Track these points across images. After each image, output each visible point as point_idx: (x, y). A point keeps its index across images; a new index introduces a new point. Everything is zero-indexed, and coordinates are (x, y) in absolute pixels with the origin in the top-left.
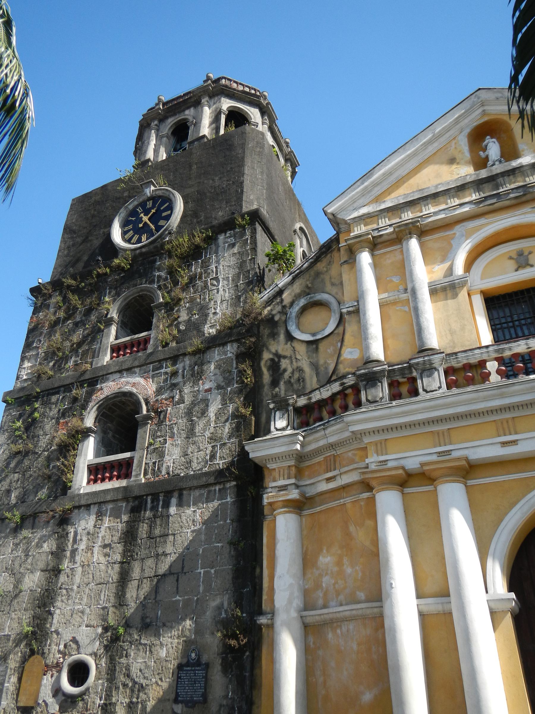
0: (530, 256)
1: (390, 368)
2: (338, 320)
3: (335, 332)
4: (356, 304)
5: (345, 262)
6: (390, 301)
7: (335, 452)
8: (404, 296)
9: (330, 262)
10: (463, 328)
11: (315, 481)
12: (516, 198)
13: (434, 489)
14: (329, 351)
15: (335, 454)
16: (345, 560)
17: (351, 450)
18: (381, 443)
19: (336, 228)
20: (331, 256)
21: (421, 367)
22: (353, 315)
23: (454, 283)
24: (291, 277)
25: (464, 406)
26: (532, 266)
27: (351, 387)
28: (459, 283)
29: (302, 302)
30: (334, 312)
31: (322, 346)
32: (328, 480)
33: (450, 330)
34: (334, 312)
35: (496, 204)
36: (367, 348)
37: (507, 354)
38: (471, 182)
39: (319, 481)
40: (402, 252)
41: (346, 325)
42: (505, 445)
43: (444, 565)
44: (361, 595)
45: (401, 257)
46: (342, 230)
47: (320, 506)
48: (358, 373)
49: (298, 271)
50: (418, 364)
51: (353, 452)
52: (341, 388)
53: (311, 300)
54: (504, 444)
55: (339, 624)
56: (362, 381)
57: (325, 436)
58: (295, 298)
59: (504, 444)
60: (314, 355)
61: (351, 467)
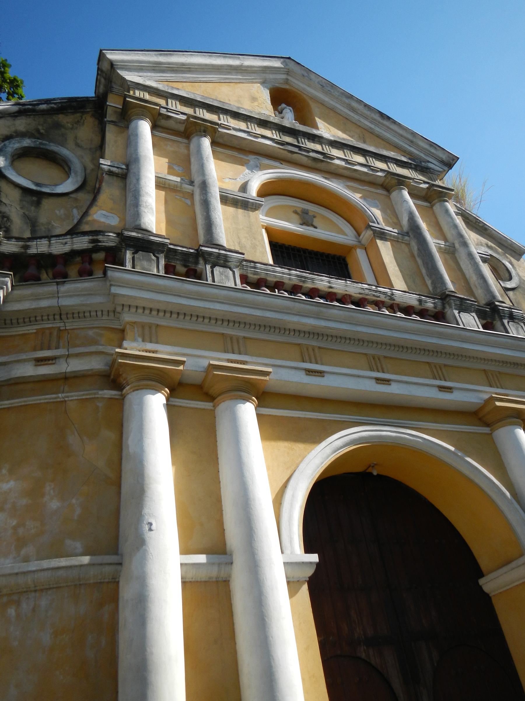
0: (315, 219)
1: (172, 247)
2: (80, 183)
3: (72, 196)
4: (124, 167)
5: (112, 122)
6: (169, 185)
7: (62, 324)
8: (187, 188)
9: (78, 122)
10: (254, 247)
11: (10, 360)
12: (315, 159)
13: (212, 408)
14: (57, 212)
15: (62, 328)
16: (48, 488)
17: (94, 328)
18: (150, 328)
19: (102, 89)
20: (82, 117)
21: (212, 259)
22: (115, 178)
23: (248, 202)
24: (16, 108)
25: (272, 313)
26: (315, 227)
27: (107, 249)
28: (253, 203)
29: (27, 142)
30: (76, 173)
31: (46, 203)
32: (40, 361)
33: (239, 243)
34: (76, 173)
35: (295, 155)
36: (137, 215)
37: (309, 285)
38: (274, 123)
39: (18, 361)
40: (188, 148)
41: (104, 184)
42: (311, 373)
43: (220, 511)
44: (78, 546)
45: (186, 152)
46: (114, 90)
47: (8, 399)
48: (127, 233)
49: (30, 107)
50: (210, 254)
51: (97, 331)
52: (91, 246)
53: (41, 146)
54: (309, 372)
55: (15, 597)
56: (128, 246)
57: (57, 295)
58: (15, 134)
59: (309, 371)
60: (33, 208)
61: (93, 349)
